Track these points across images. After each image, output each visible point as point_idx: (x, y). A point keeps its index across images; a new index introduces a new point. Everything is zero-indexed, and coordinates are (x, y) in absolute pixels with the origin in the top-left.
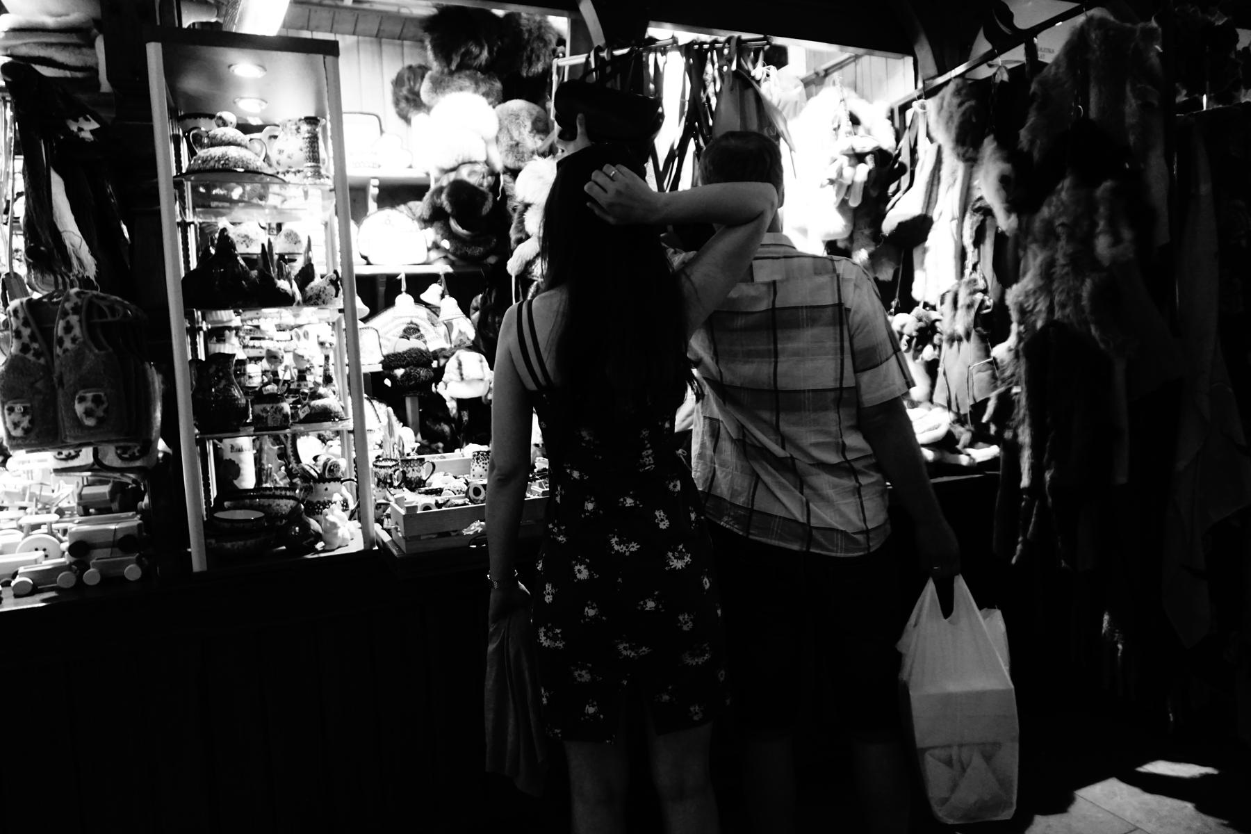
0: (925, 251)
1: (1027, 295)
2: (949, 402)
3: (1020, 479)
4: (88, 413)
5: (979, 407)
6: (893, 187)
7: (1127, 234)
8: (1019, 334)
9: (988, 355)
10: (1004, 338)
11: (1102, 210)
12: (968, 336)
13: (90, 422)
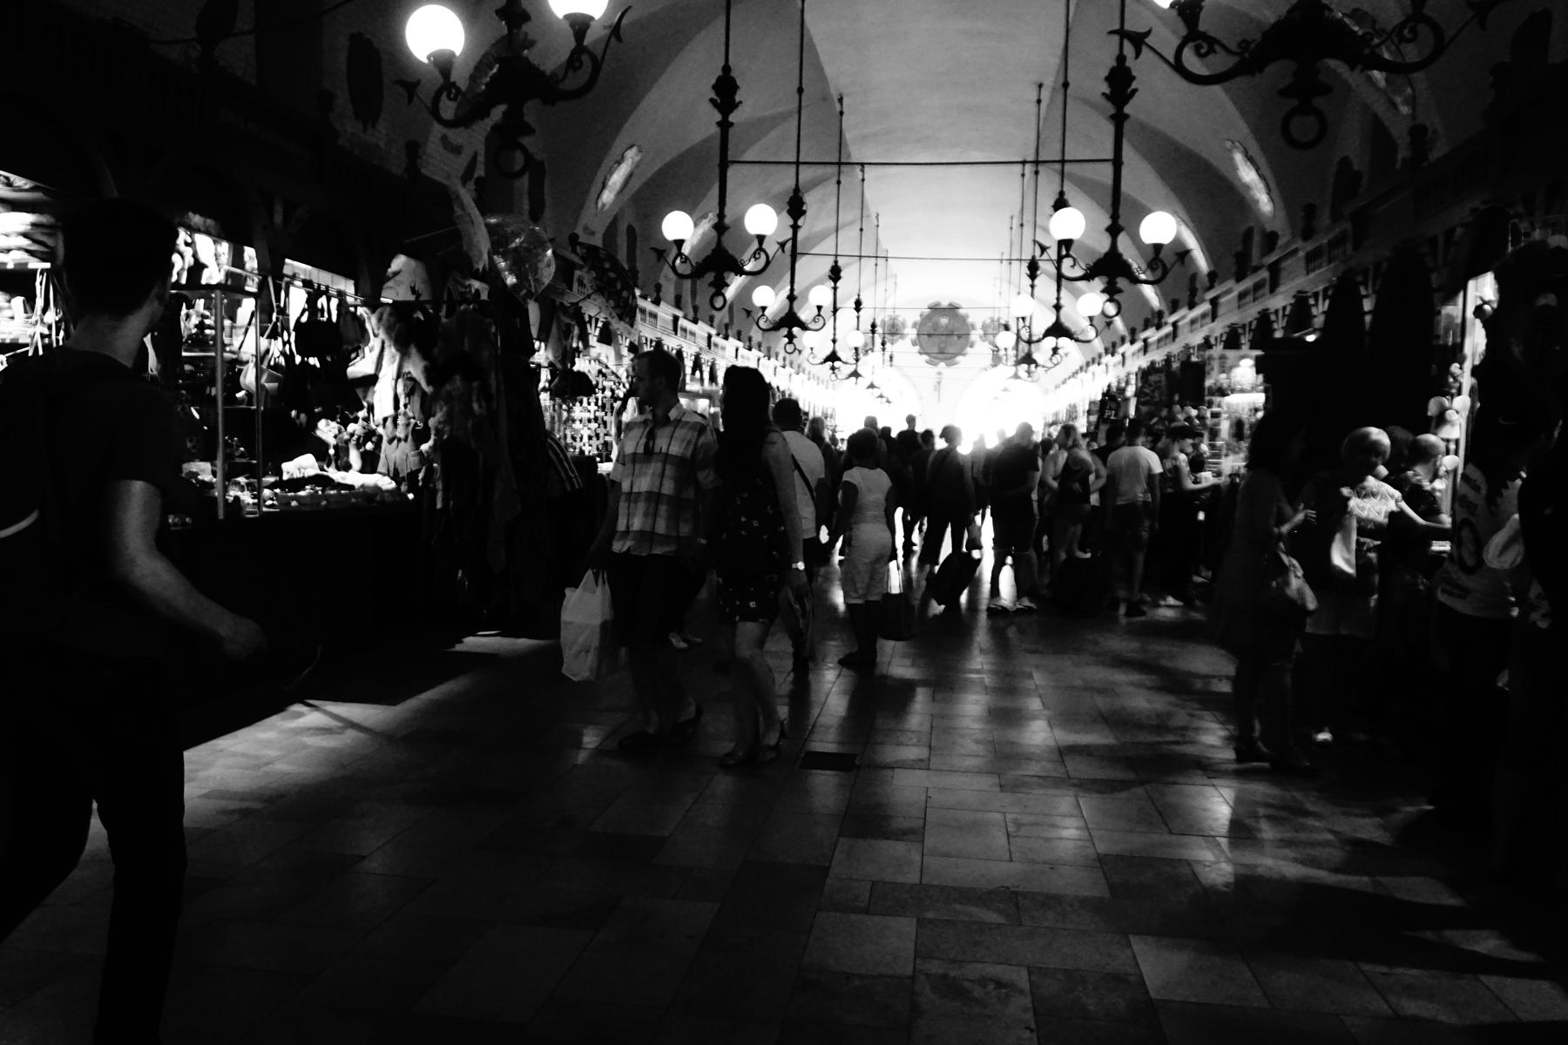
0: (374, 392)
1: (440, 422)
2: (388, 471)
3: (436, 505)
4: (194, 447)
5: (413, 475)
6: (353, 355)
7: (484, 404)
8: (435, 441)
10: (427, 442)
11: (475, 392)
12: (406, 440)
13: (193, 451)
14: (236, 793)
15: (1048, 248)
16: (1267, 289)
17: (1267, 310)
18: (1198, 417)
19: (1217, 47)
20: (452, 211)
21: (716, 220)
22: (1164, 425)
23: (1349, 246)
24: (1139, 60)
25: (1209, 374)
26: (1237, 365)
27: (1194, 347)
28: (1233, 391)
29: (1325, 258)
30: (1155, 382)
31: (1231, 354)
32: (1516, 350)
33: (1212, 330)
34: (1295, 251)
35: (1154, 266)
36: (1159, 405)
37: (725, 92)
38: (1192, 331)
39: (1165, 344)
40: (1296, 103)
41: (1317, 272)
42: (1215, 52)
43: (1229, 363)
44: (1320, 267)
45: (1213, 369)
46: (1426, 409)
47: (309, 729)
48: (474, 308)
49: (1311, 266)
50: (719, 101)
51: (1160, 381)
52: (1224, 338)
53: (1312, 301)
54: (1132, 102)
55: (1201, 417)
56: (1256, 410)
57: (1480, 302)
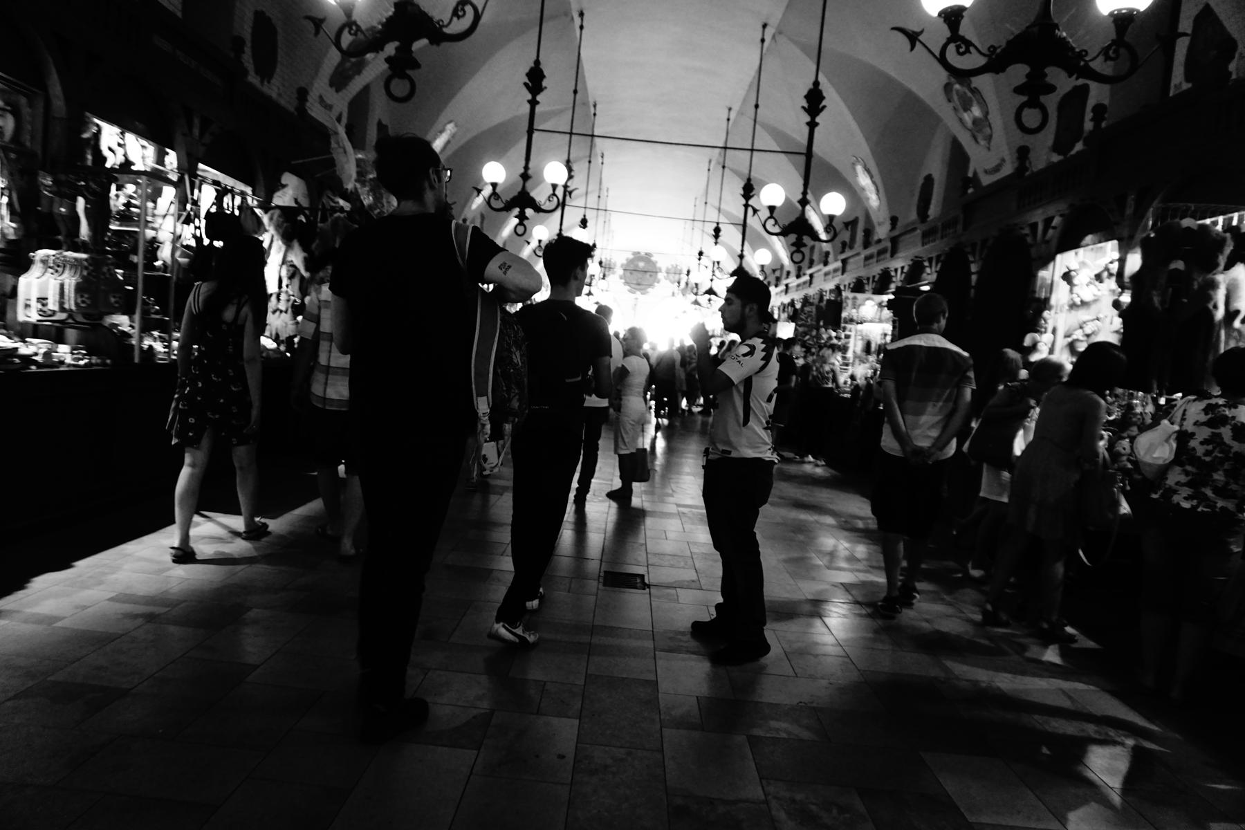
2: (271, 334)
4: (116, 302)
5: (290, 339)
9: (295, 319)
13: (117, 305)
14: (144, 597)
15: (758, 210)
16: (888, 255)
17: (888, 268)
18: (836, 338)
19: (972, 49)
20: (330, 143)
21: (522, 171)
22: (813, 341)
23: (960, 227)
24: (913, 52)
25: (845, 308)
26: (863, 304)
27: (826, 292)
28: (865, 322)
29: (939, 235)
30: (808, 312)
31: (859, 296)
32: (1156, 300)
33: (842, 280)
34: (914, 229)
35: (828, 230)
36: (811, 328)
37: (535, 80)
38: (825, 280)
39: (803, 289)
40: (1024, 99)
41: (933, 244)
42: (970, 53)
43: (858, 302)
44: (934, 241)
45: (847, 305)
46: (1022, 341)
47: (204, 538)
48: (345, 216)
49: (926, 240)
50: (530, 84)
51: (811, 312)
52: (851, 286)
53: (926, 264)
54: (821, 114)
55: (838, 338)
56: (885, 335)
57: (1067, 270)
